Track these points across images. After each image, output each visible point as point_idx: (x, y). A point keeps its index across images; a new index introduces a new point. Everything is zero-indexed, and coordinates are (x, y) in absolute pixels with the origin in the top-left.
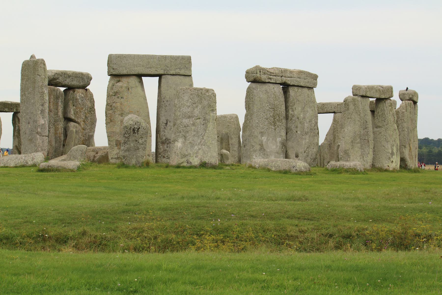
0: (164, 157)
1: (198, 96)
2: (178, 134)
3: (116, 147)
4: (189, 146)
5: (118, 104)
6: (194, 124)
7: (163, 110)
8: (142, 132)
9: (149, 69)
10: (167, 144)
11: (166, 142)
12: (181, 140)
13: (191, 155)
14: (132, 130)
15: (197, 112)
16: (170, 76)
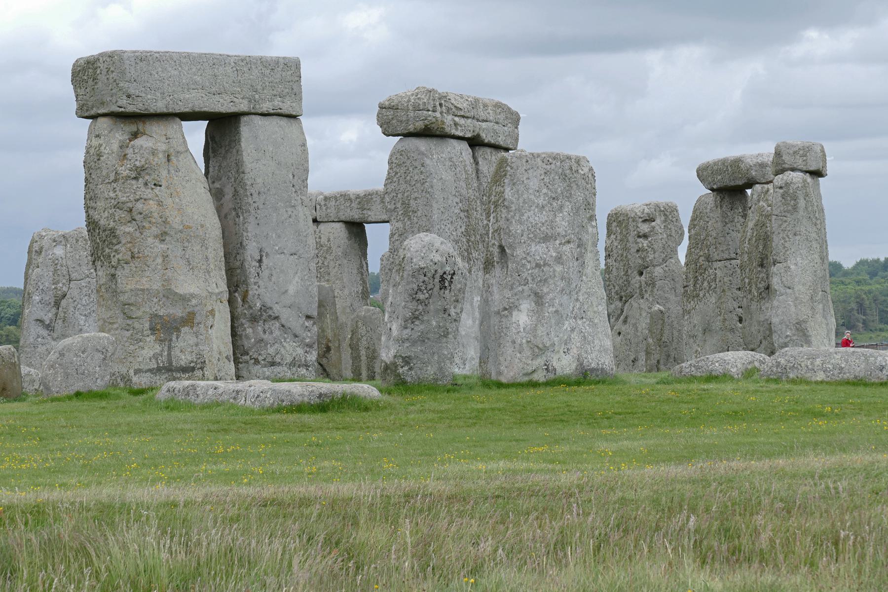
0: (257, 362)
1: (564, 177)
2: (520, 288)
3: (152, 338)
4: (553, 321)
5: (152, 205)
6: (559, 259)
7: (251, 219)
8: (459, 286)
9: (217, 97)
10: (265, 321)
11: (261, 315)
12: (526, 305)
13: (556, 349)
14: (437, 280)
15: (562, 223)
16: (258, 117)
